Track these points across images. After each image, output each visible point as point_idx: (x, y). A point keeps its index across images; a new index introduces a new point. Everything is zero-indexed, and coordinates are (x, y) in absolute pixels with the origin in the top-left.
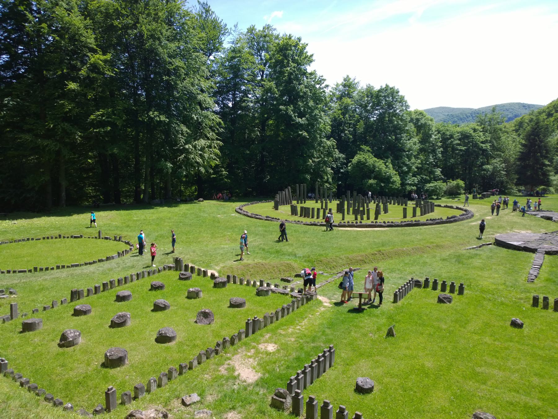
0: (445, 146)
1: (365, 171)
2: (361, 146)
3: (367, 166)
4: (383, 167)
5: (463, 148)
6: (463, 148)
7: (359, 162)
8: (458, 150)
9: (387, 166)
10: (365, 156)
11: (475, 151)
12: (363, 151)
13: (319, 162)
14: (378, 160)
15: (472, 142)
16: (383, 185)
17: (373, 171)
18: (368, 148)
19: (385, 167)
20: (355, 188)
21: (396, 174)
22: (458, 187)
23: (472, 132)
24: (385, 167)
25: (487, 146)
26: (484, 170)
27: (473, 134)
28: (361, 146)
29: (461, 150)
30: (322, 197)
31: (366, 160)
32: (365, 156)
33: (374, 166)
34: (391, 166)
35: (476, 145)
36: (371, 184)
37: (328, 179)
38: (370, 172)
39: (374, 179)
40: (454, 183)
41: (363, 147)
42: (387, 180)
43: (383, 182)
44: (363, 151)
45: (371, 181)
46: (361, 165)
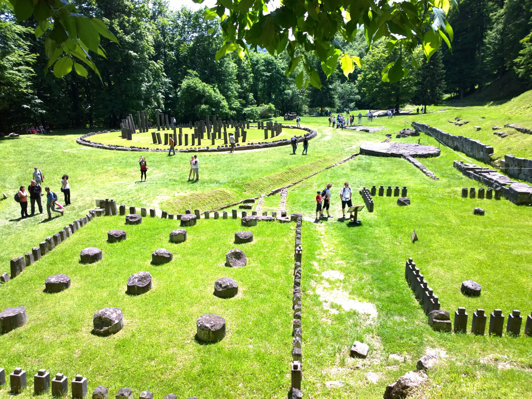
0: (256, 72)
1: (195, 96)
2: (188, 71)
4: (211, 91)
5: (269, 74)
6: (269, 74)
8: (264, 75)
9: (214, 90)
10: (192, 81)
11: (278, 77)
12: (191, 75)
13: (150, 86)
14: (206, 85)
15: (275, 68)
16: (214, 110)
18: (195, 72)
19: (211, 91)
20: (190, 113)
21: (223, 99)
22: (270, 110)
24: (211, 91)
26: (286, 94)
27: (275, 61)
28: (188, 71)
29: (267, 76)
30: (163, 124)
31: (195, 84)
32: (192, 81)
33: (204, 91)
34: (218, 90)
35: (278, 72)
36: (204, 110)
37: (159, 103)
38: (201, 97)
40: (266, 107)
41: (190, 71)
42: (217, 104)
43: (214, 108)
44: (191, 75)
45: (203, 106)
46: (191, 90)
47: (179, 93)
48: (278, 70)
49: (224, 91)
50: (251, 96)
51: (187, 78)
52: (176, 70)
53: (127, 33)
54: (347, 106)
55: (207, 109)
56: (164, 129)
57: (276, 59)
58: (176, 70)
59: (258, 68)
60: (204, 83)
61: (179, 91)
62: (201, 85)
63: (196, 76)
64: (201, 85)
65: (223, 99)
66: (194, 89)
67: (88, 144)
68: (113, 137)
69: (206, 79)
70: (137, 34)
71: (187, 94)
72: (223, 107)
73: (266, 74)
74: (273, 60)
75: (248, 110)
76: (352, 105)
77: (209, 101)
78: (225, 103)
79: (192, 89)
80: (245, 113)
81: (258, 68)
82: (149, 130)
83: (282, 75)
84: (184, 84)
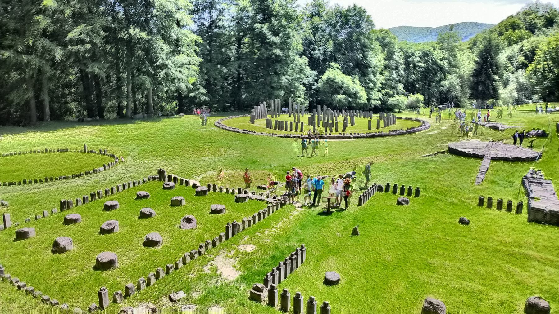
0: (407, 64)
1: (334, 87)
6: (423, 65)
8: (418, 66)
9: (354, 82)
10: (334, 73)
11: (434, 69)
17: (341, 87)
18: (337, 65)
19: (352, 83)
22: (418, 101)
23: (432, 49)
25: (444, 63)
27: (433, 52)
34: (357, 82)
35: (435, 63)
39: (344, 93)
41: (332, 64)
42: (355, 95)
45: (341, 97)
46: (330, 82)
53: (276, 34)
54: (529, 97)
57: (434, 49)
63: (338, 68)
69: (347, 72)
70: (285, 34)
71: (326, 85)
73: (419, 64)
76: (535, 97)
83: (438, 66)
84: (324, 77)
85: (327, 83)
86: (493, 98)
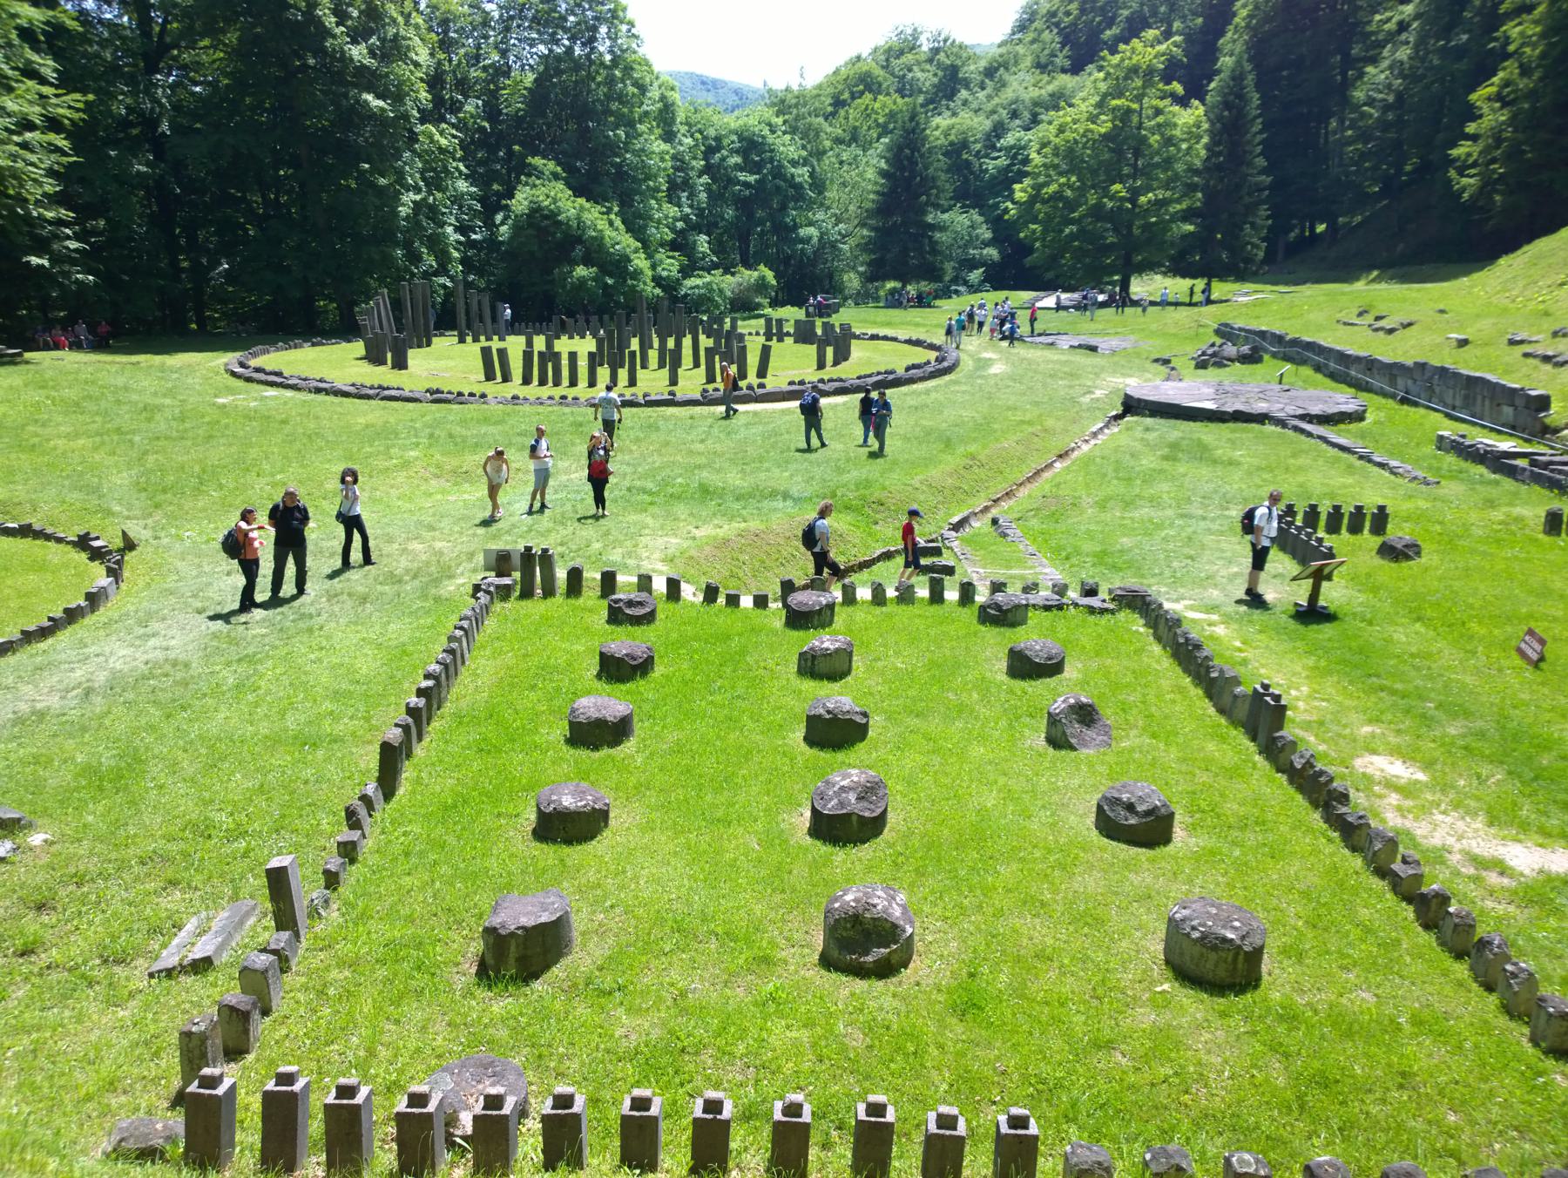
2: (529, 159)
3: (560, 223)
7: (536, 211)
10: (545, 191)
11: (778, 188)
15: (772, 160)
17: (579, 240)
22: (761, 286)
23: (766, 132)
25: (802, 174)
27: (770, 139)
28: (529, 159)
30: (477, 324)
32: (545, 191)
35: (778, 172)
36: (582, 281)
39: (587, 262)
40: (747, 276)
41: (537, 161)
42: (617, 266)
45: (581, 271)
46: (541, 221)
47: (504, 229)
48: (781, 166)
49: (636, 225)
50: (703, 243)
51: (527, 184)
52: (498, 153)
55: (593, 279)
56: (476, 340)
57: (773, 132)
58: (498, 153)
59: (723, 159)
60: (581, 201)
61: (503, 223)
62: (570, 206)
63: (556, 176)
64: (570, 206)
65: (636, 251)
66: (552, 216)
67: (276, 380)
68: (341, 361)
69: (580, 189)
71: (530, 231)
72: (637, 274)
74: (764, 137)
75: (697, 287)
77: (595, 253)
78: (640, 262)
79: (546, 217)
80: (686, 295)
81: (723, 159)
82: (435, 340)
84: (521, 201)
85: (530, 225)
86: (895, 278)
